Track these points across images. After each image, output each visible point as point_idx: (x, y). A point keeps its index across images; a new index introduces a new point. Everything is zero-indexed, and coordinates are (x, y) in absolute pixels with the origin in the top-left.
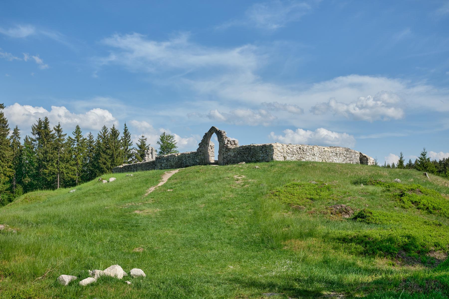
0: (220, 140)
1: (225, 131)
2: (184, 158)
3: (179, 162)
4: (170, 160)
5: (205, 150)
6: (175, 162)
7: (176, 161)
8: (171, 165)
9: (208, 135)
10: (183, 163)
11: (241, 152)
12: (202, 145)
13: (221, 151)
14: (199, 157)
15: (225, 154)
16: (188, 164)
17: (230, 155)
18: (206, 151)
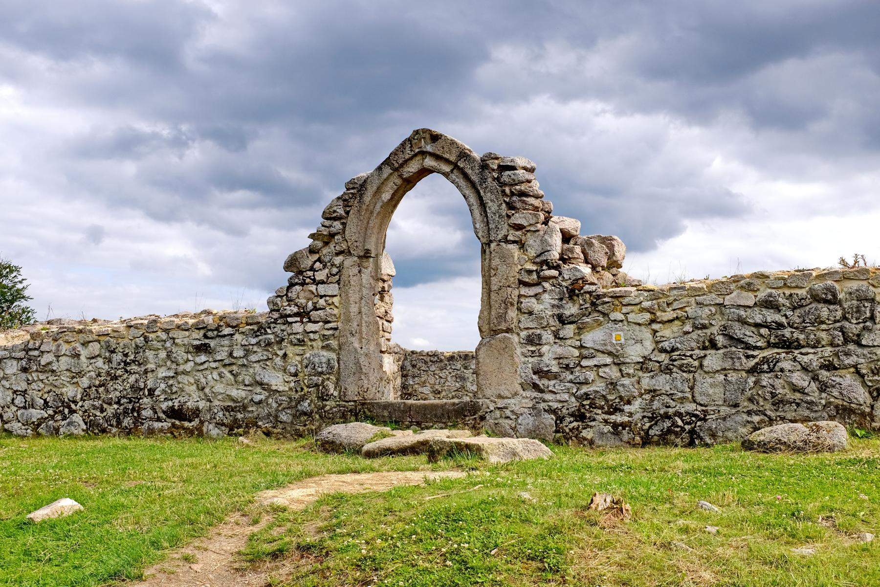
0: (503, 232)
1: (533, 164)
2: (163, 354)
3: (115, 378)
4: (50, 363)
5: (346, 303)
6: (85, 382)
7: (99, 375)
8: (59, 397)
9: (378, 191)
10: (151, 392)
11: (739, 331)
12: (312, 269)
13: (512, 313)
14: (291, 350)
15: (547, 336)
16: (193, 400)
17: (609, 348)
18: (354, 309)
